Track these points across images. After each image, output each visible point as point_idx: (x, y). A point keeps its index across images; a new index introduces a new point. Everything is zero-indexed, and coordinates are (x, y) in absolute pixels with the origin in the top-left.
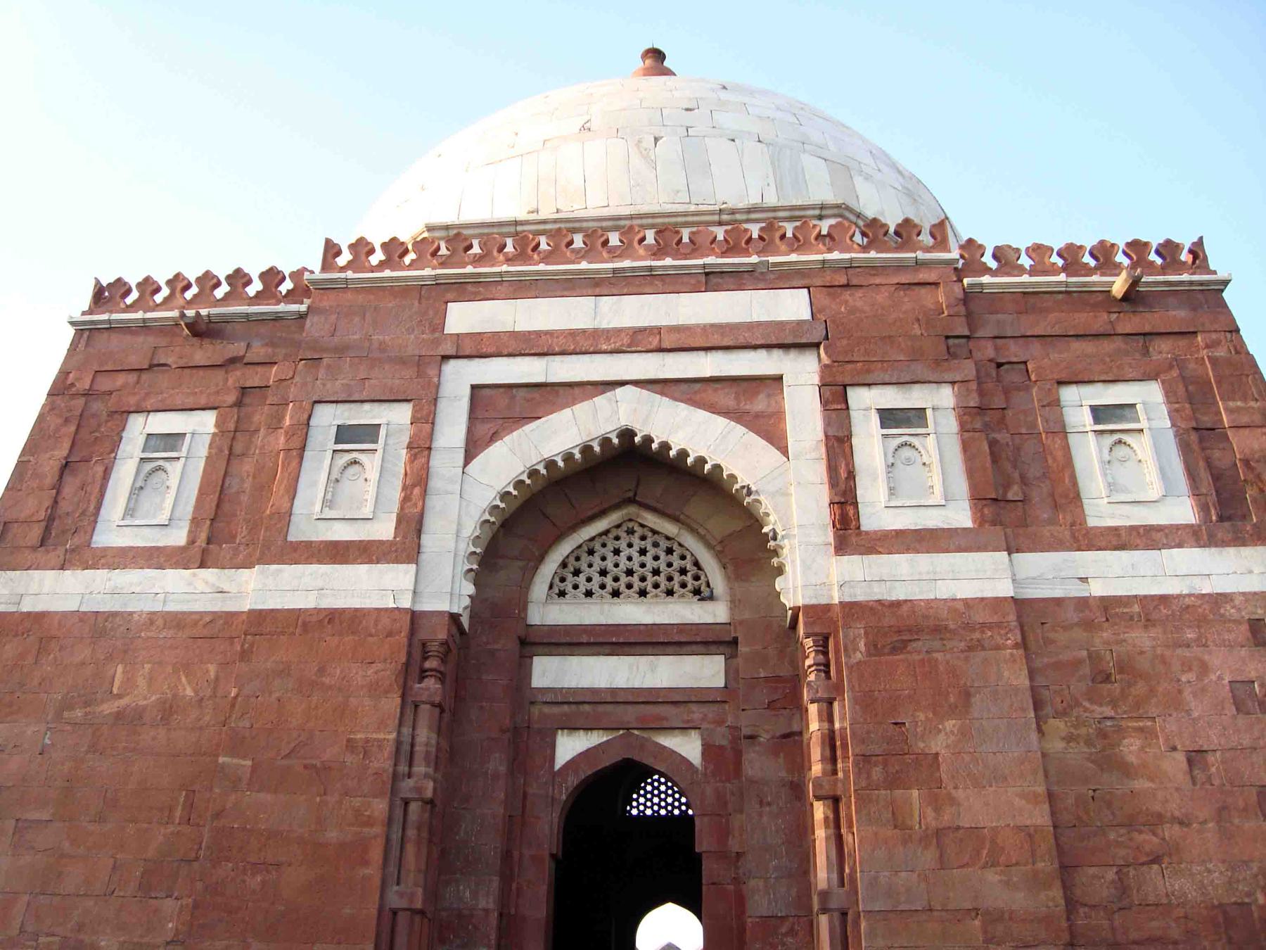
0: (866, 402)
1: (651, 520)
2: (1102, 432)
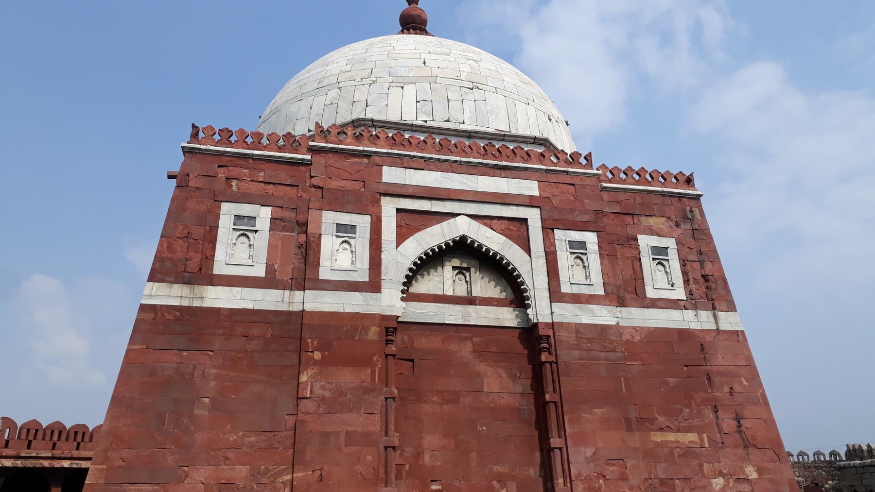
0: (561, 236)
2: (654, 259)
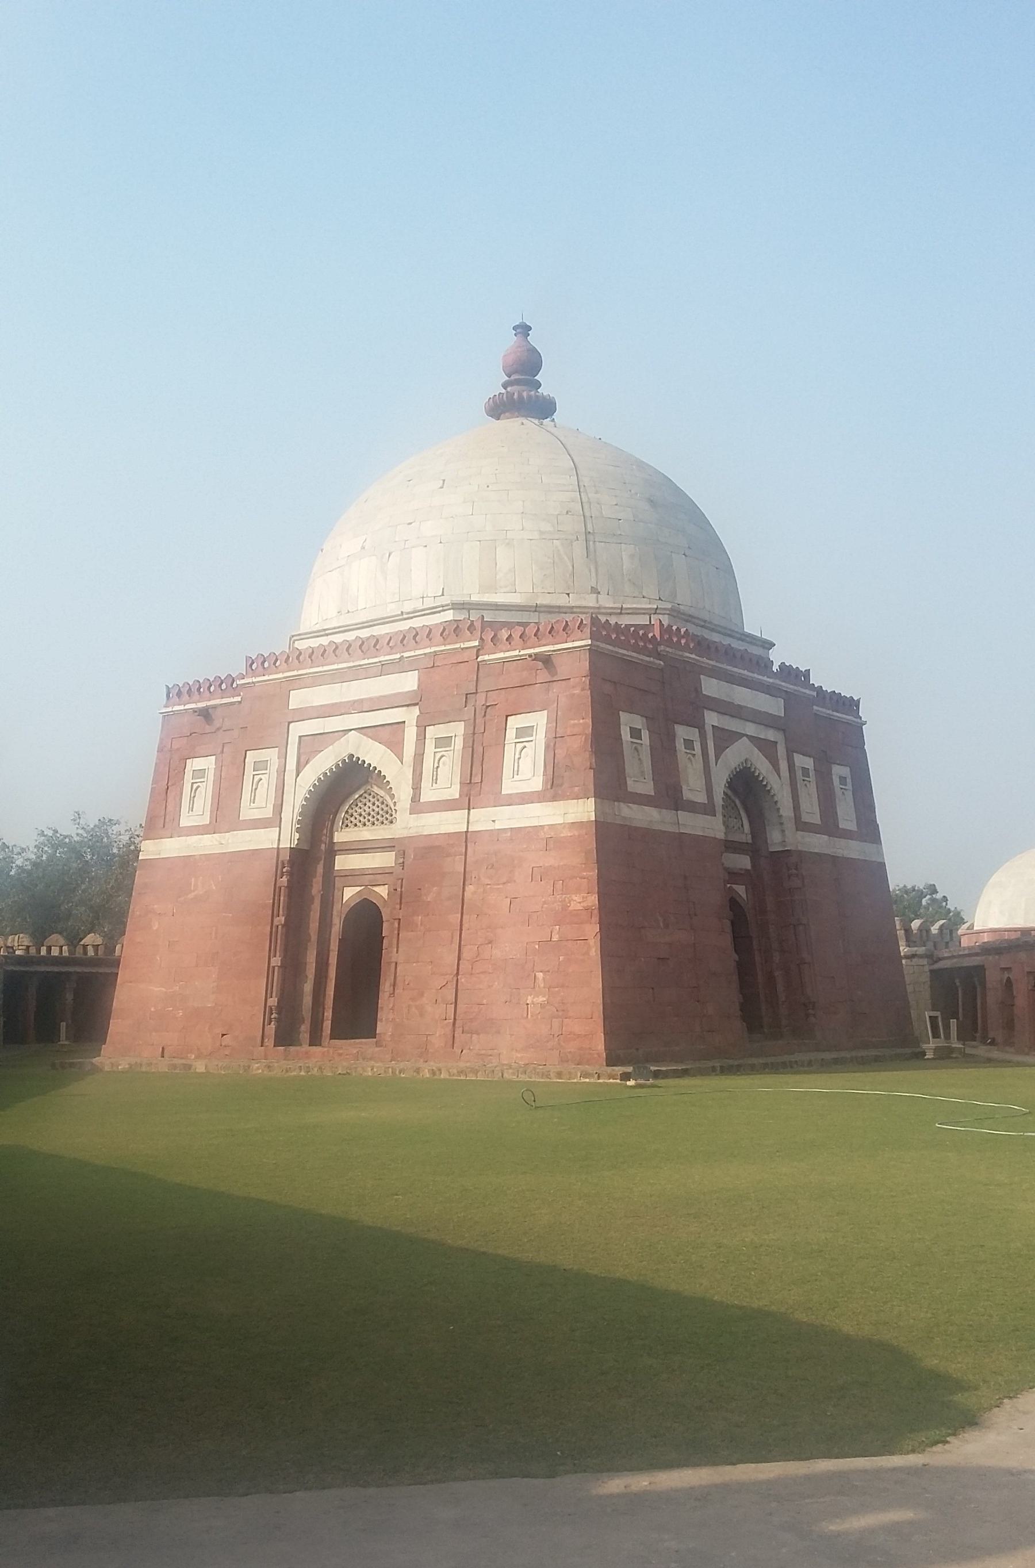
1: (376, 789)
